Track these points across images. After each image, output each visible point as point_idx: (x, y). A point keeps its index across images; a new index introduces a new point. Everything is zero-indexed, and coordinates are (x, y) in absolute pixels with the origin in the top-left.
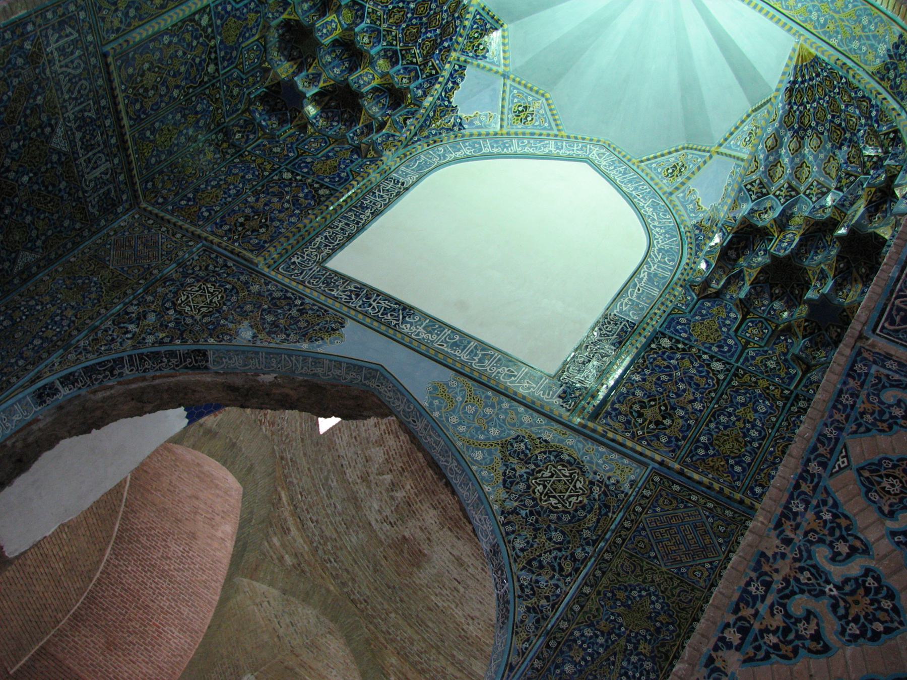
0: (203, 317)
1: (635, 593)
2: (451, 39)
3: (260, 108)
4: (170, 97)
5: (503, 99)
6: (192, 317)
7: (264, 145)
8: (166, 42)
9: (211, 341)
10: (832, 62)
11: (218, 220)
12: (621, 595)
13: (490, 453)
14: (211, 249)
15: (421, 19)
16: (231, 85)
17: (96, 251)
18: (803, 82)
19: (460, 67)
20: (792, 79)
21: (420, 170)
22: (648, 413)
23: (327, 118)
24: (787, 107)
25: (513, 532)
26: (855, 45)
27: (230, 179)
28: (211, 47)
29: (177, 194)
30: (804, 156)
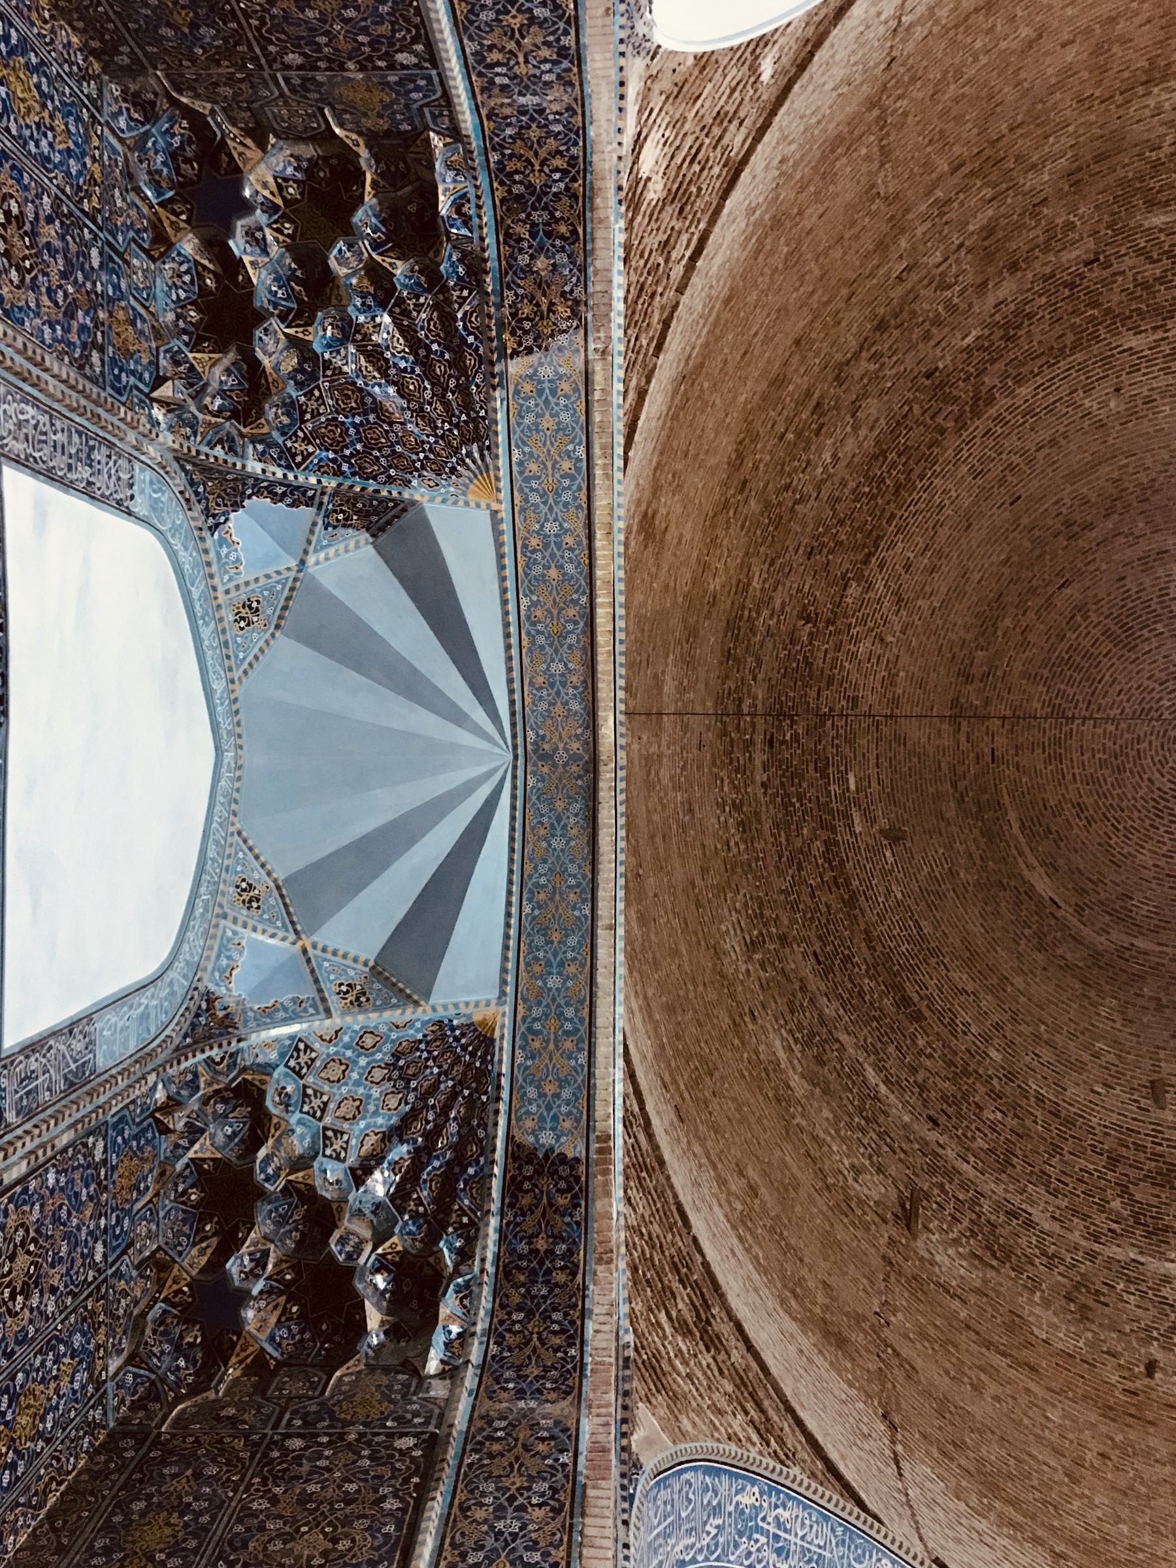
2: (354, 474)
18: (457, 1039)
20: (455, 1022)
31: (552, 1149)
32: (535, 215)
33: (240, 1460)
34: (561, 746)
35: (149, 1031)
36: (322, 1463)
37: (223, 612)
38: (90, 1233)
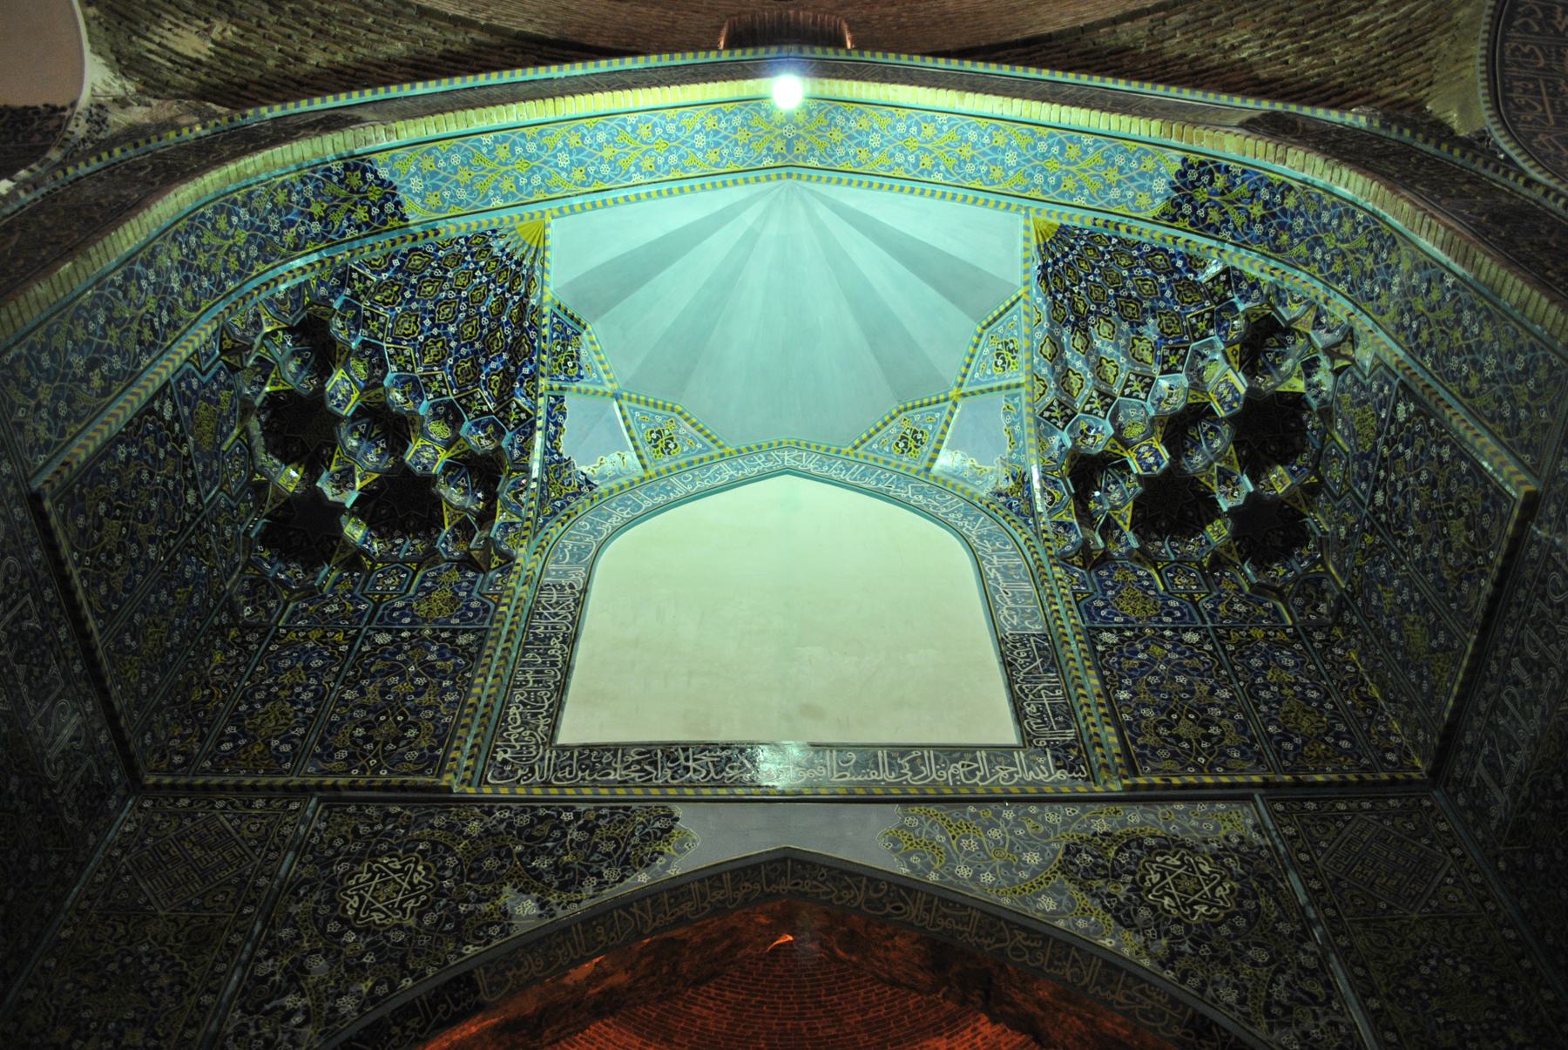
0: (420, 916)
1: (1425, 970)
2: (531, 362)
3: (266, 554)
4: (146, 562)
5: (628, 429)
6: (400, 927)
7: (305, 610)
8: (122, 457)
9: (470, 950)
10: (1088, 224)
11: (318, 750)
12: (1414, 983)
13: (1061, 892)
14: (340, 799)
15: (472, 345)
16: (221, 521)
17: (107, 898)
18: (1055, 263)
19: (556, 398)
21: (580, 559)
22: (1183, 729)
23: (381, 536)
24: (1049, 299)
25: (1204, 983)
26: (1115, 193)
27: (286, 678)
28: (186, 458)
29: (202, 738)
30: (1098, 351)
31: (1171, 183)
32: (275, 227)
33: (1381, 545)
34: (778, 132)
35: (1019, 567)
36: (1400, 487)
37: (662, 468)
38: (1174, 649)
